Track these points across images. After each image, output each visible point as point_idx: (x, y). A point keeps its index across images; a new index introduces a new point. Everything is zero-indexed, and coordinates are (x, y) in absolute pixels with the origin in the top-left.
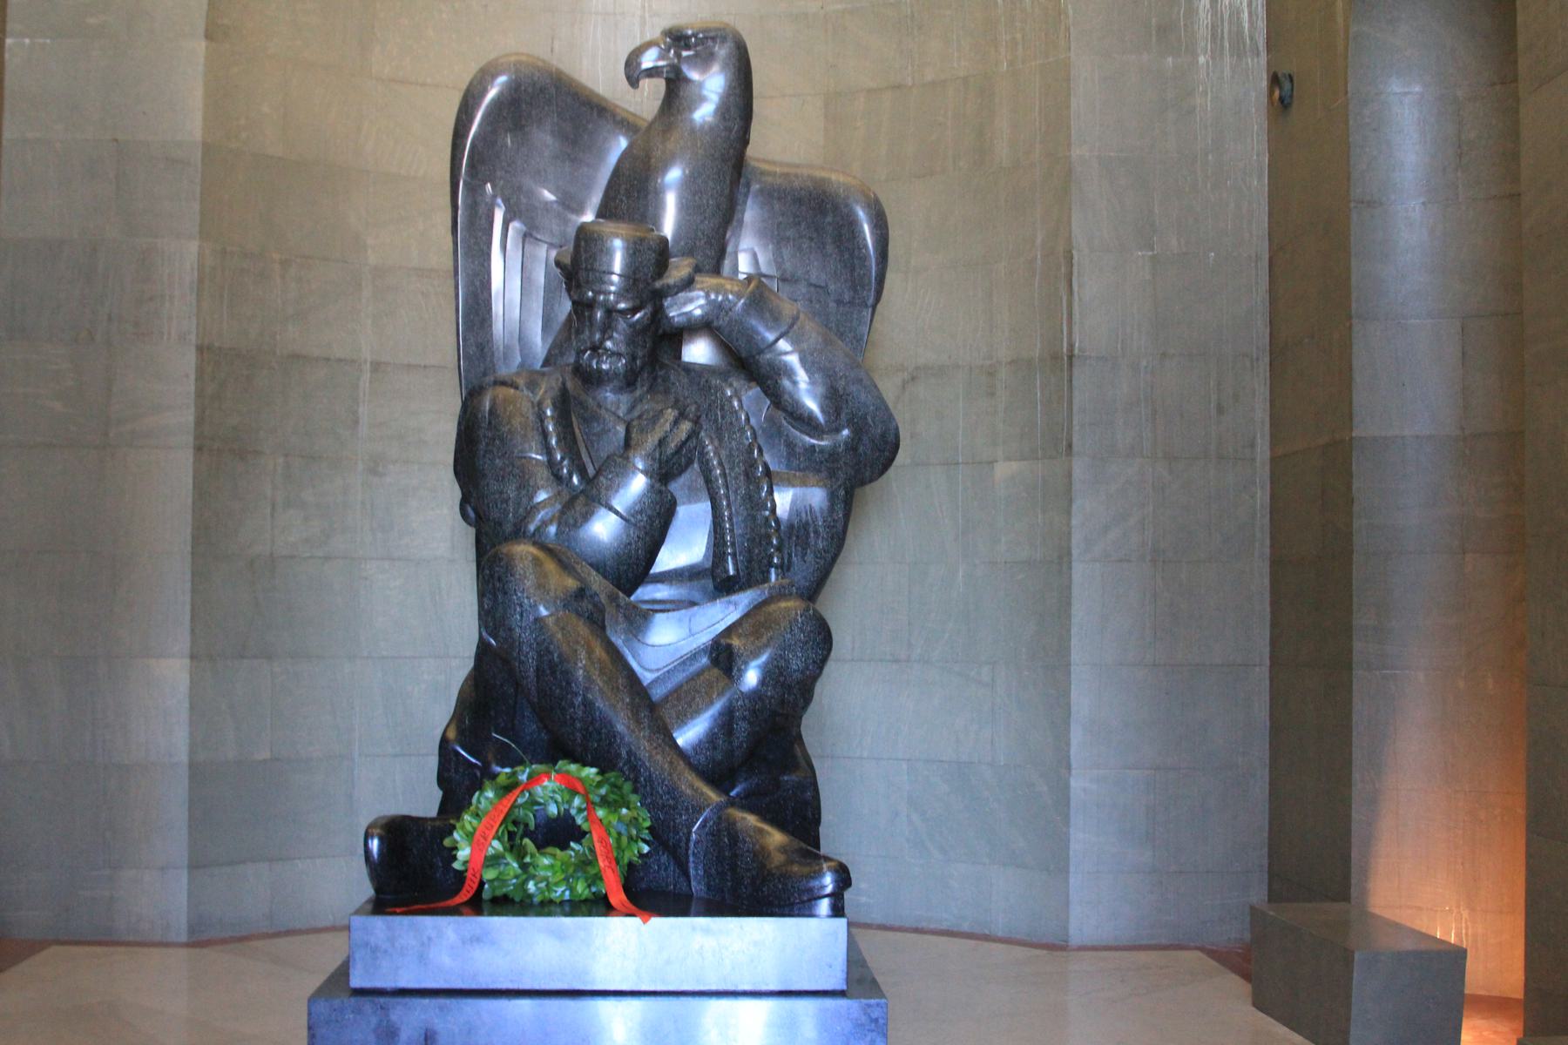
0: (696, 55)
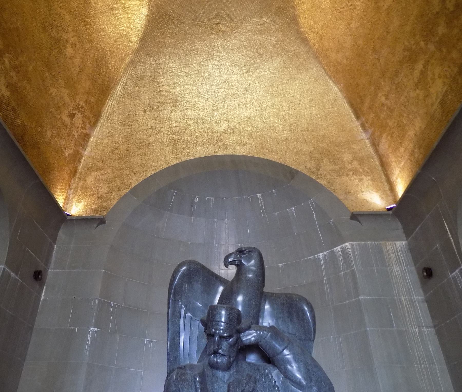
0: (246, 256)
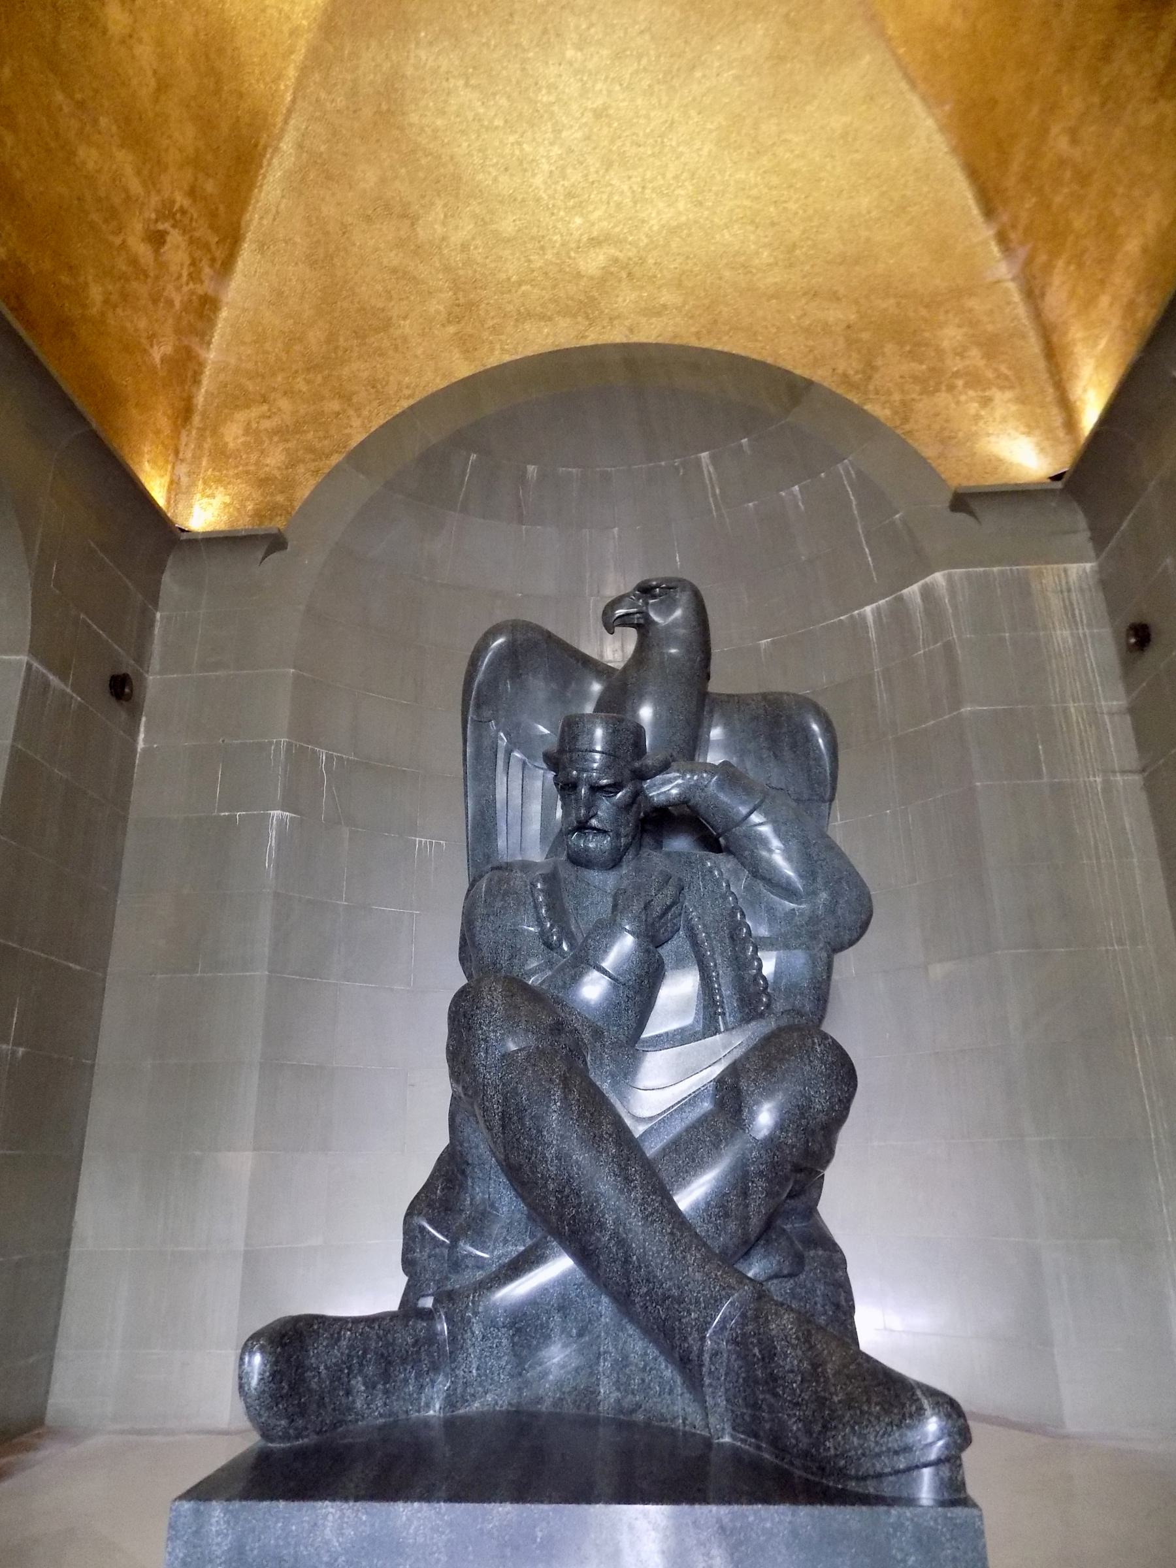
0: (662, 602)
